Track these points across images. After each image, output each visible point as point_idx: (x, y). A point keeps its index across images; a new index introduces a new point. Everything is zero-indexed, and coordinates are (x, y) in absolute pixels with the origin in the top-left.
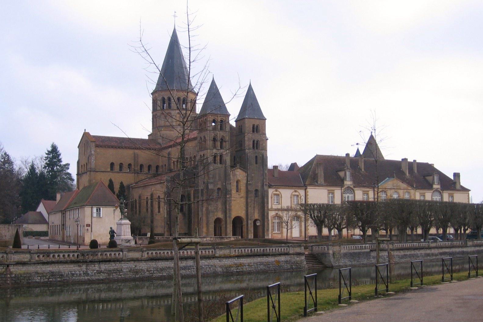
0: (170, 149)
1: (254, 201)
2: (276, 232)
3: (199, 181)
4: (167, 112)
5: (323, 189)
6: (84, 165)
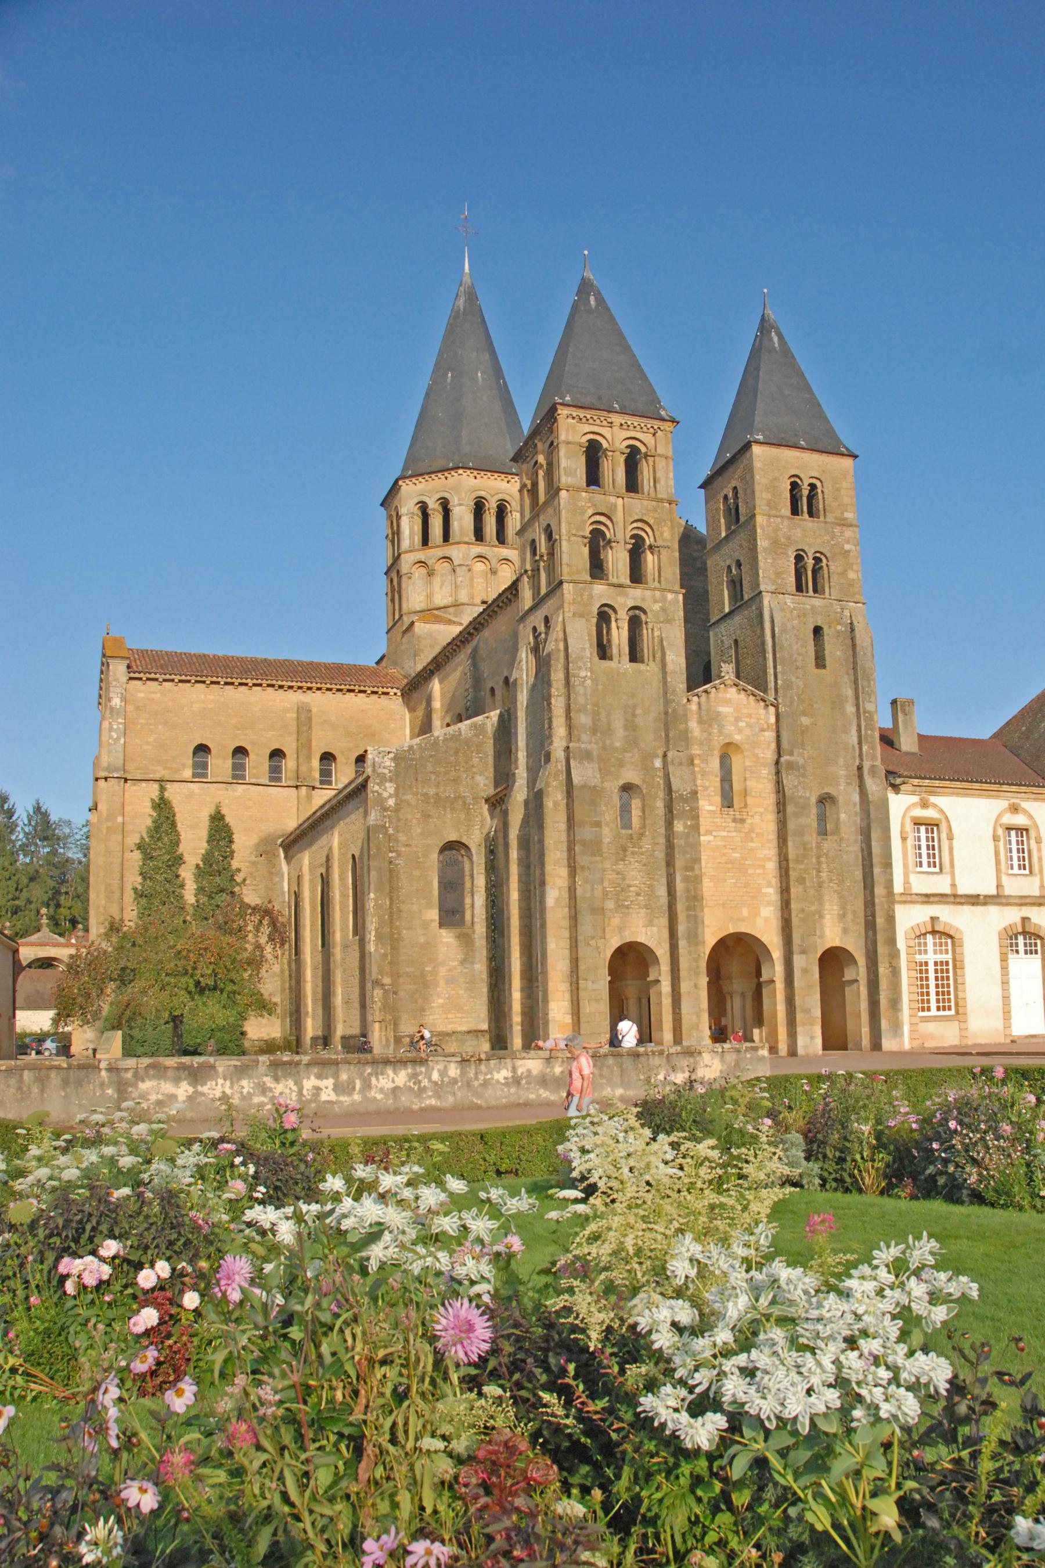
1: (818, 857)
2: (934, 1012)
4: (440, 552)
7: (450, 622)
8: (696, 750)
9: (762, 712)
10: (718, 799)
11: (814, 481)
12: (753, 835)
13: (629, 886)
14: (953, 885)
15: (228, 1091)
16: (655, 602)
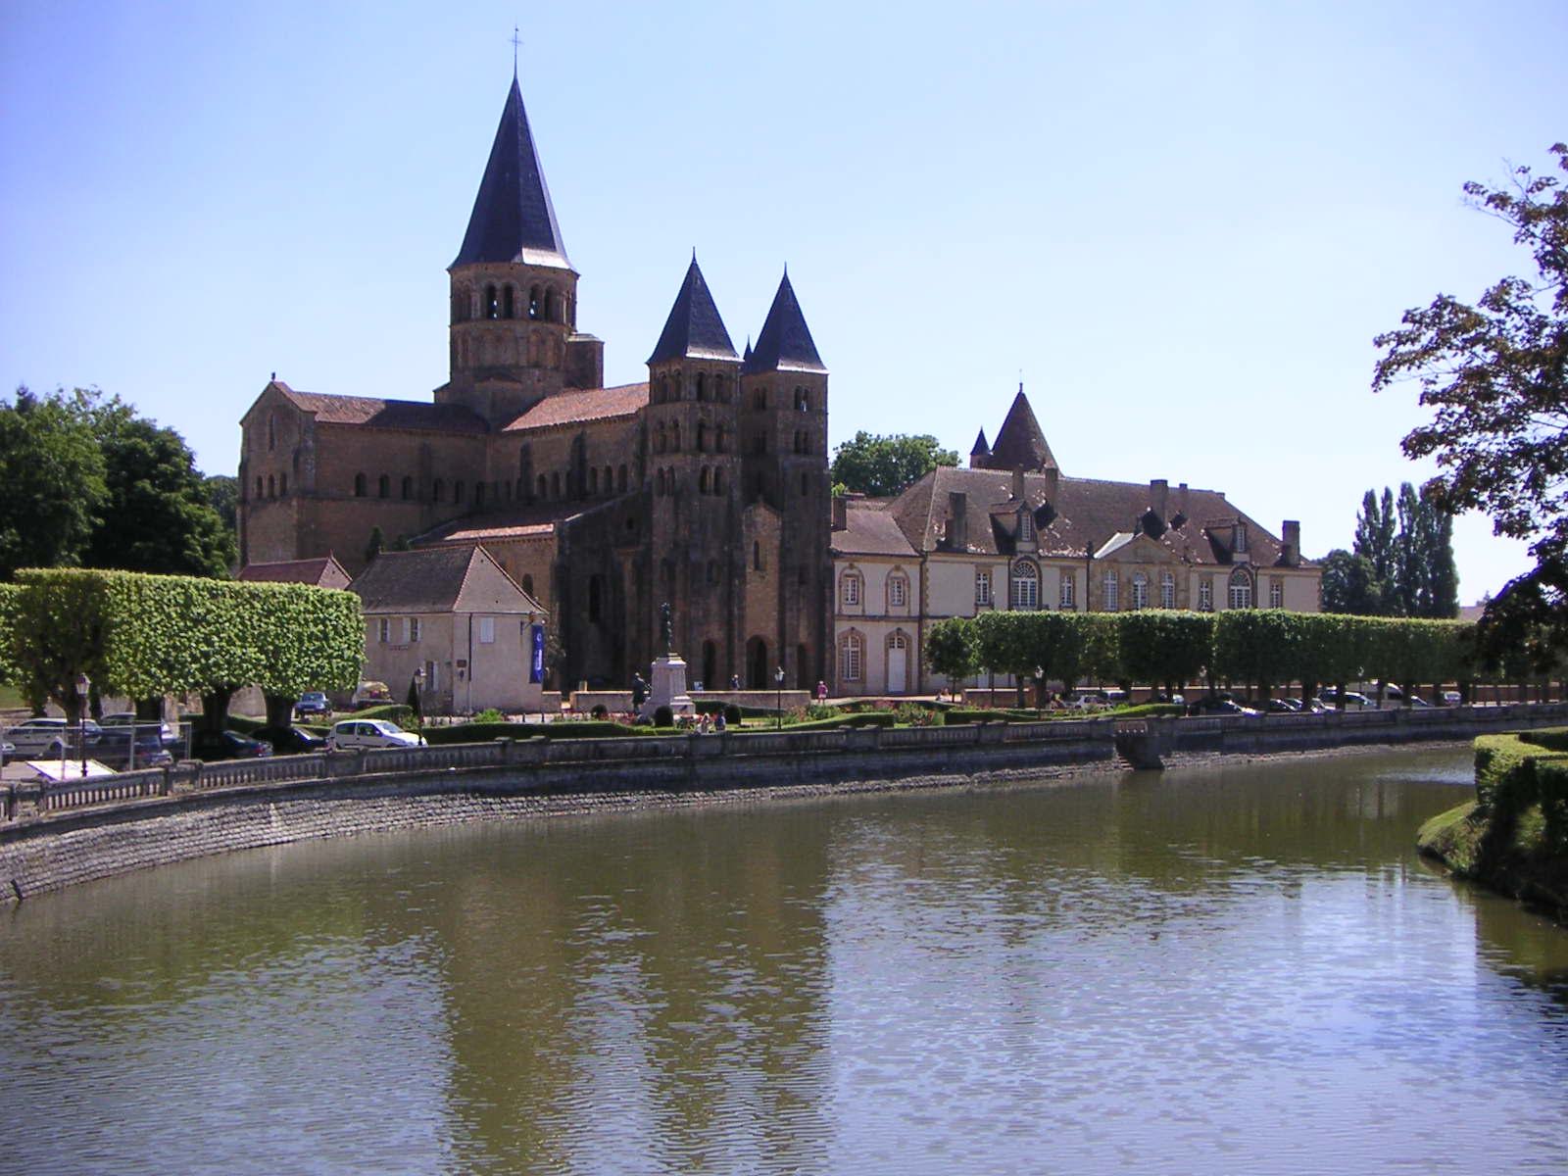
0: (528, 439)
3: (655, 539)
4: (506, 324)
5: (966, 563)
6: (271, 480)
7: (513, 380)
14: (863, 611)
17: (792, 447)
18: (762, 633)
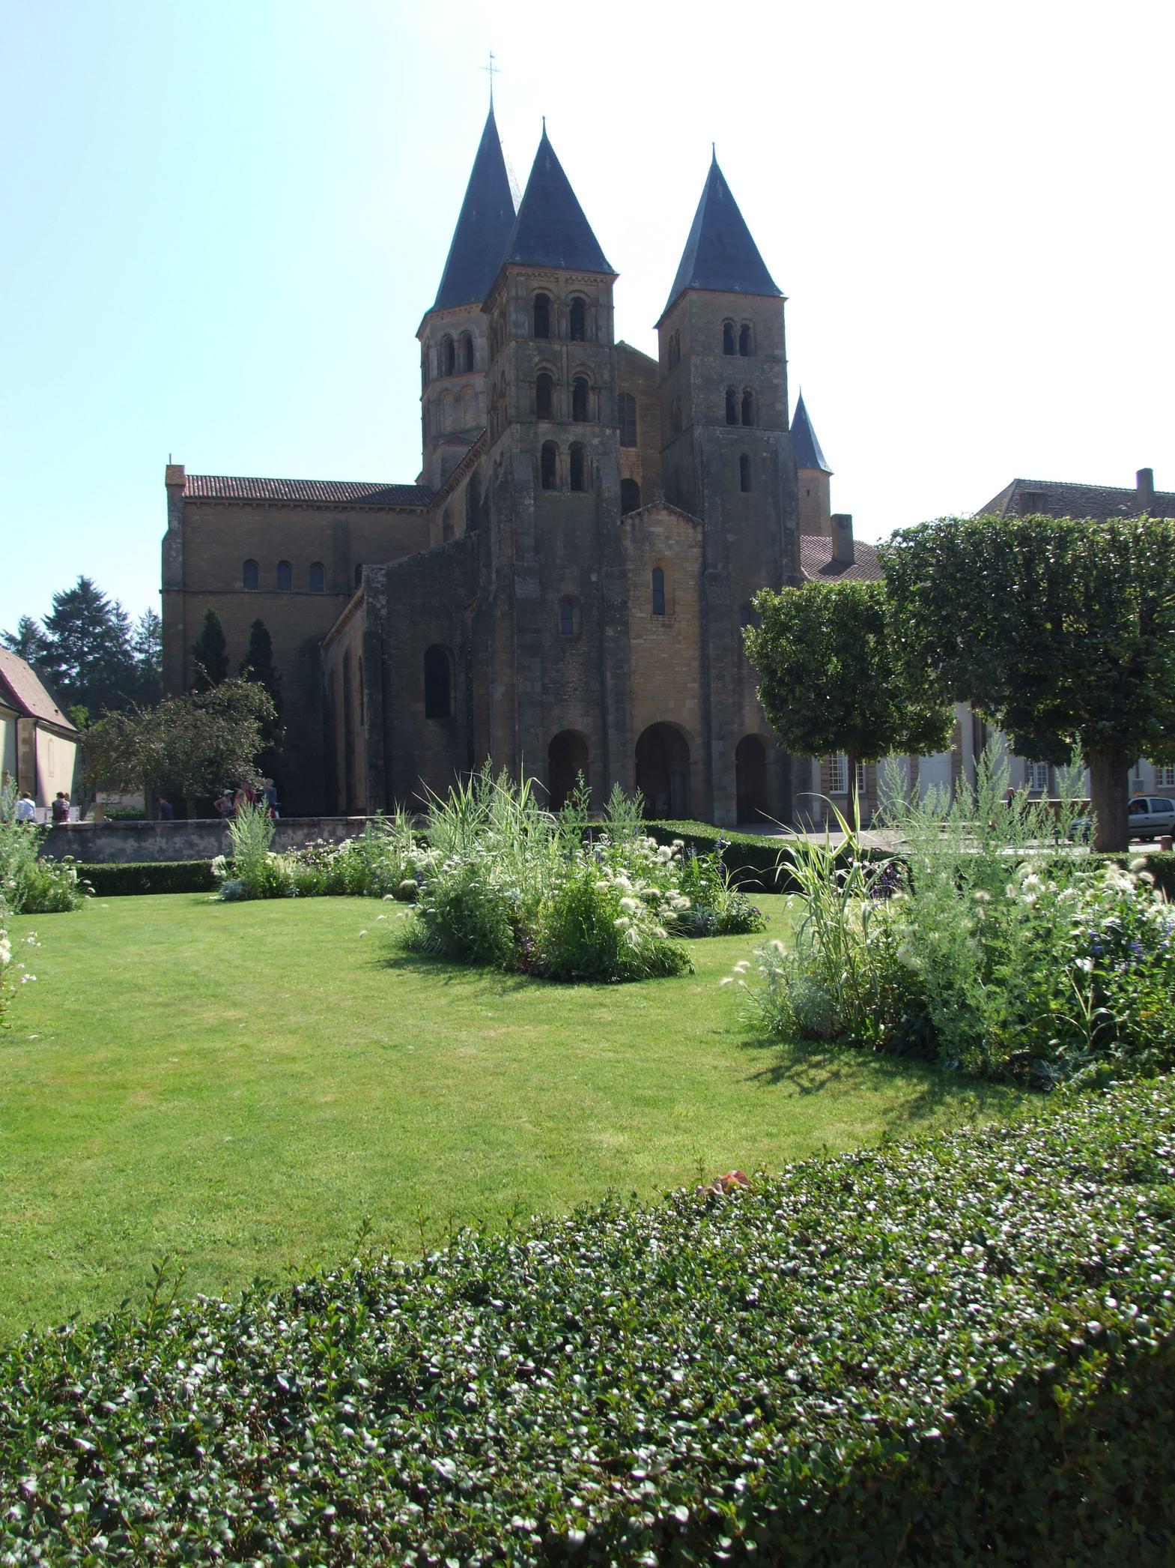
8: (630, 566)
9: (691, 531)
10: (650, 607)
11: (747, 322)
12: (680, 638)
13: (568, 682)
15: (164, 846)
16: (595, 436)
17: (722, 412)
18: (669, 718)
